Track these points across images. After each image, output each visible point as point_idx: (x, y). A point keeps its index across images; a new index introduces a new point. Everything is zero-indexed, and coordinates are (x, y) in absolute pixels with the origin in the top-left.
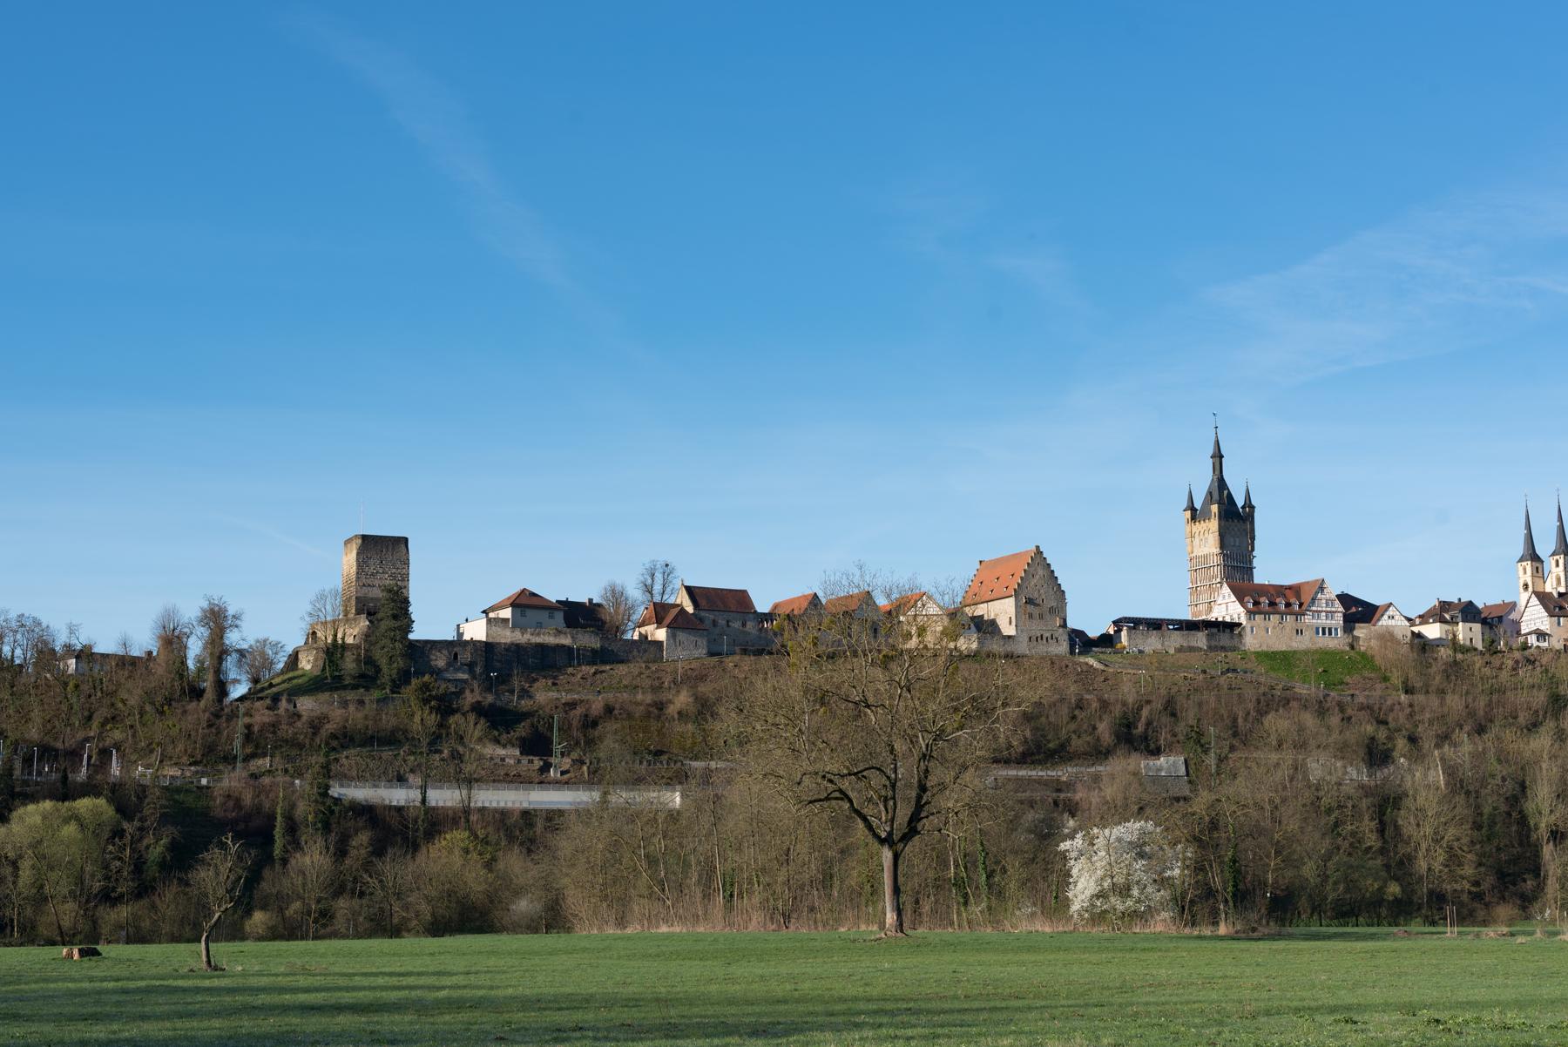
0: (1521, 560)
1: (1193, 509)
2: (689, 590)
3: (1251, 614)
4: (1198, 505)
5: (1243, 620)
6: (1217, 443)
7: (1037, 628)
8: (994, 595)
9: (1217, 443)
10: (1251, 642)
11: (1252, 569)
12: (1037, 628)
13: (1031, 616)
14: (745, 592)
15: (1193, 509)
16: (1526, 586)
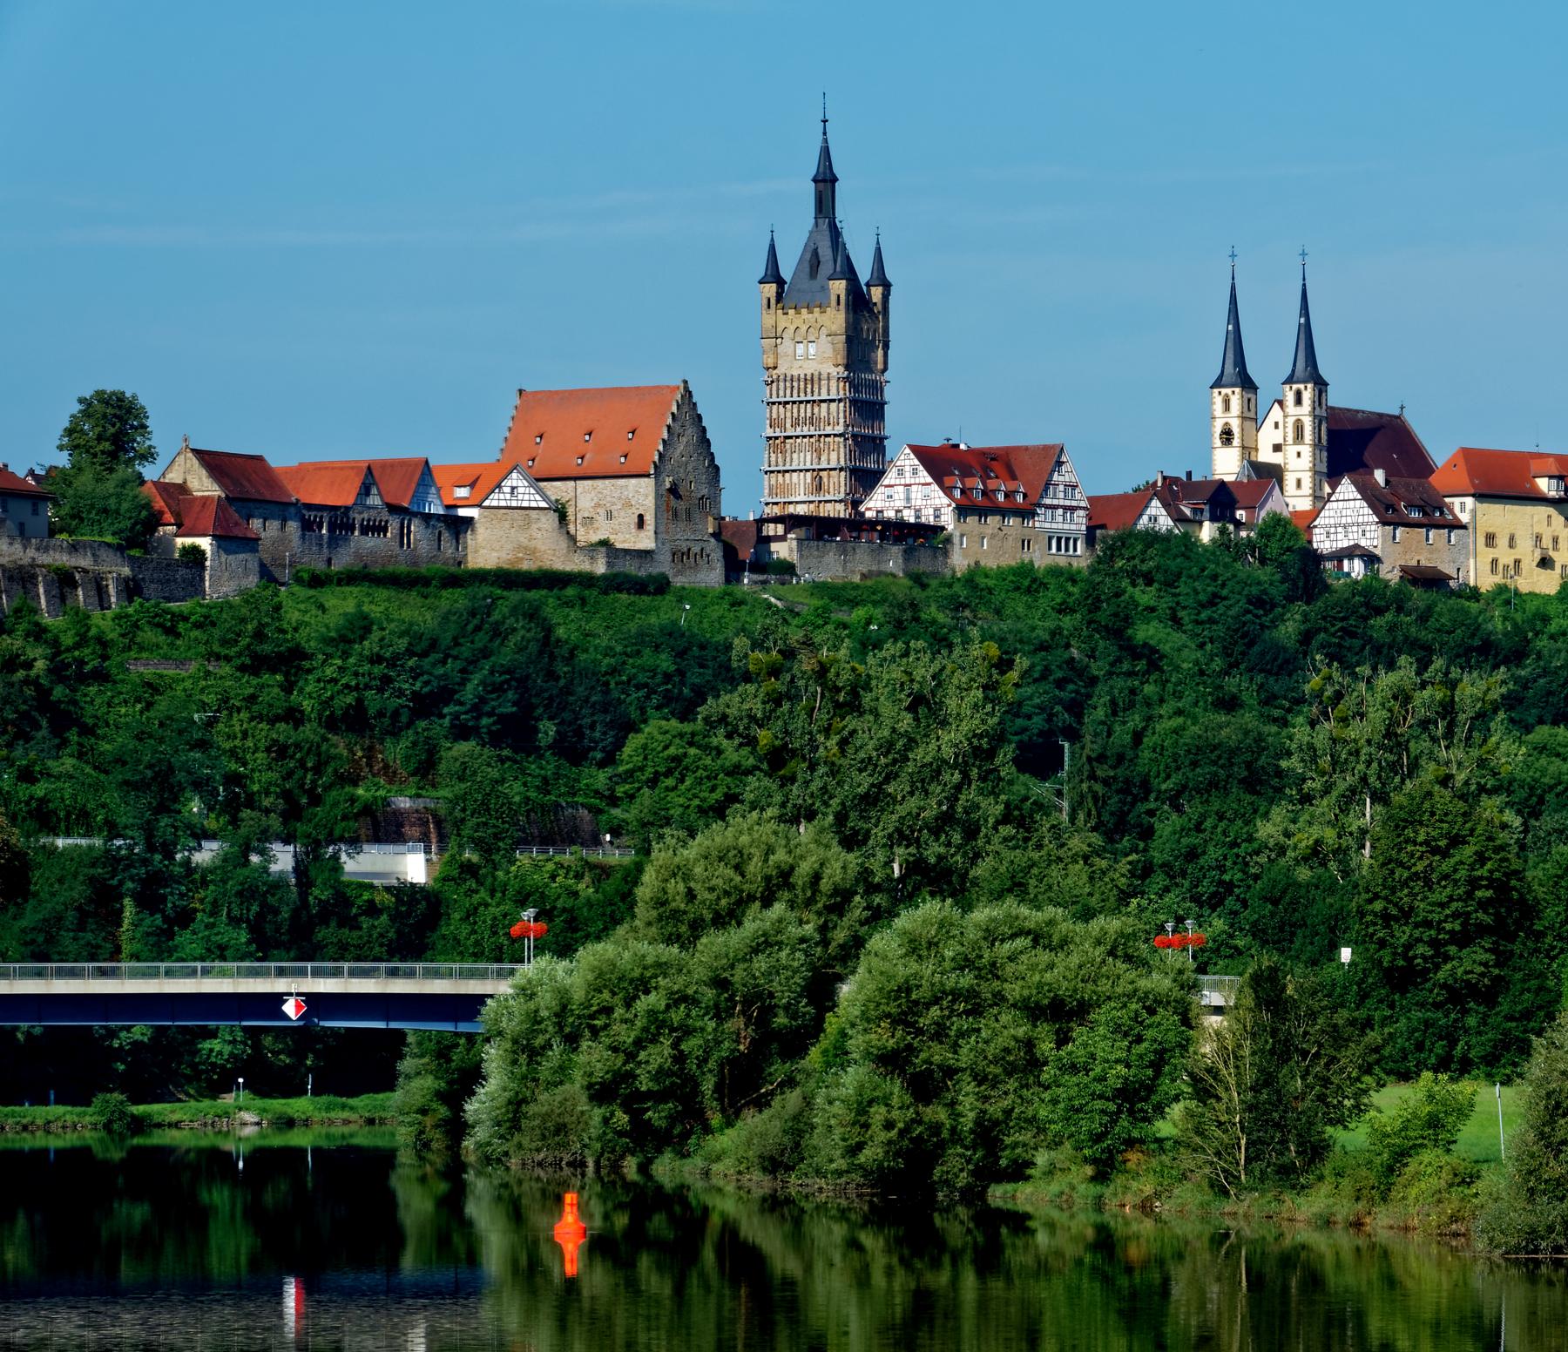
0: (1218, 384)
1: (773, 275)
2: (213, 462)
3: (962, 511)
4: (786, 272)
5: (948, 519)
6: (826, 153)
7: (683, 536)
8: (588, 465)
9: (826, 153)
10: (959, 561)
11: (883, 404)
12: (683, 536)
13: (676, 515)
14: (260, 459)
15: (773, 275)
16: (1227, 436)
